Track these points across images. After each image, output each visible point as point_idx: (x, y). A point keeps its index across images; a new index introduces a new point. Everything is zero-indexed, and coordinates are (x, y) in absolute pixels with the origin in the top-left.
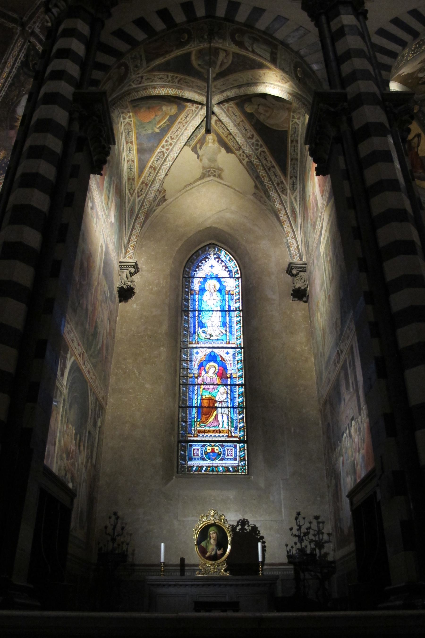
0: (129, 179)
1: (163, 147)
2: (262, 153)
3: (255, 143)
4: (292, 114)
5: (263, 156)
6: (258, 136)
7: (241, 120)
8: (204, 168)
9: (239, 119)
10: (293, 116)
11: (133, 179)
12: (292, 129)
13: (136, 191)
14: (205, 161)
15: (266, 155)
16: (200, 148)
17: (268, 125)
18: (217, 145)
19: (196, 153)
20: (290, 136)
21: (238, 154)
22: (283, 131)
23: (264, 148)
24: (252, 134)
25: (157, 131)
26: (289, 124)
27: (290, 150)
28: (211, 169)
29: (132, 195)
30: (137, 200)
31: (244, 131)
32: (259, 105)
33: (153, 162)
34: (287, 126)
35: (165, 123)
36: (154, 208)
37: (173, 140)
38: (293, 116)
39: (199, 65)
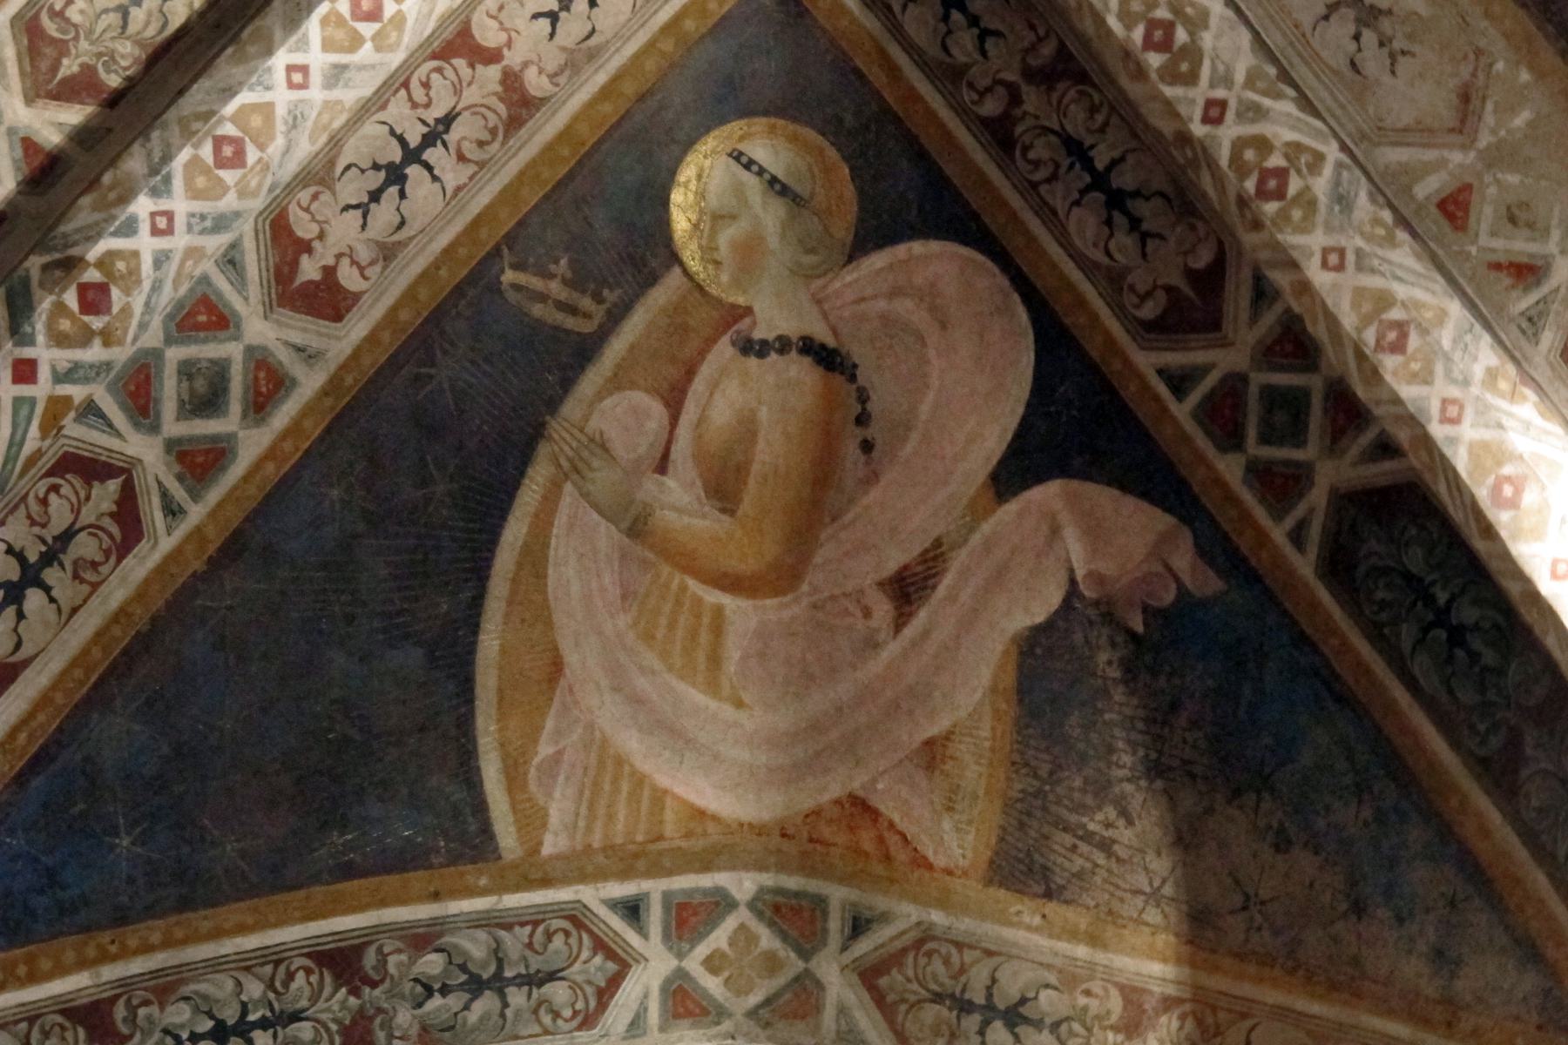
2: (106, 494)
3: (232, 351)
4: (743, 884)
5: (60, 514)
6: (333, 387)
7: (535, 82)
9: (553, 61)
10: (721, 903)
12: (533, 917)
15: (88, 575)
17: (514, 532)
20: (422, 912)
22: (471, 779)
23: (173, 511)
24: (349, 278)
26: (579, 867)
27: (215, 965)
31: (373, 142)
32: (827, 358)
34: (551, 845)
38: (721, 903)
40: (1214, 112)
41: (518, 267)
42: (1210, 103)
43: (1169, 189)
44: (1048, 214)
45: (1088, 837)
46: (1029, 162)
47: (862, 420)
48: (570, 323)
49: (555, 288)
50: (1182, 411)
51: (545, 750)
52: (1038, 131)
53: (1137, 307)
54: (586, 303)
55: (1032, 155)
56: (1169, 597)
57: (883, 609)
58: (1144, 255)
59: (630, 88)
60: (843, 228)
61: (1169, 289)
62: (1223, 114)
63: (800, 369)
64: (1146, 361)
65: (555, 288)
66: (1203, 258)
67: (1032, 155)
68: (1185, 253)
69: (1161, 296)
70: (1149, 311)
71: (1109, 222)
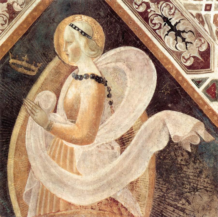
7: (17, 8)
32: (98, 79)
40: (208, 8)
41: (14, 58)
42: (207, 5)
43: (193, 30)
44: (159, 38)
45: (177, 208)
46: (153, 24)
47: (109, 96)
48: (29, 73)
49: (24, 63)
50: (200, 91)
51: (27, 189)
52: (155, 15)
53: (185, 62)
54: (33, 67)
55: (153, 22)
56: (198, 142)
57: (117, 147)
58: (187, 48)
59: (42, 8)
60: (102, 44)
61: (194, 57)
62: (211, 8)
63: (92, 83)
64: (189, 77)
65: (24, 63)
66: (204, 48)
67: (153, 22)
68: (198, 47)
69: (192, 59)
70: (188, 64)
71: (176, 40)
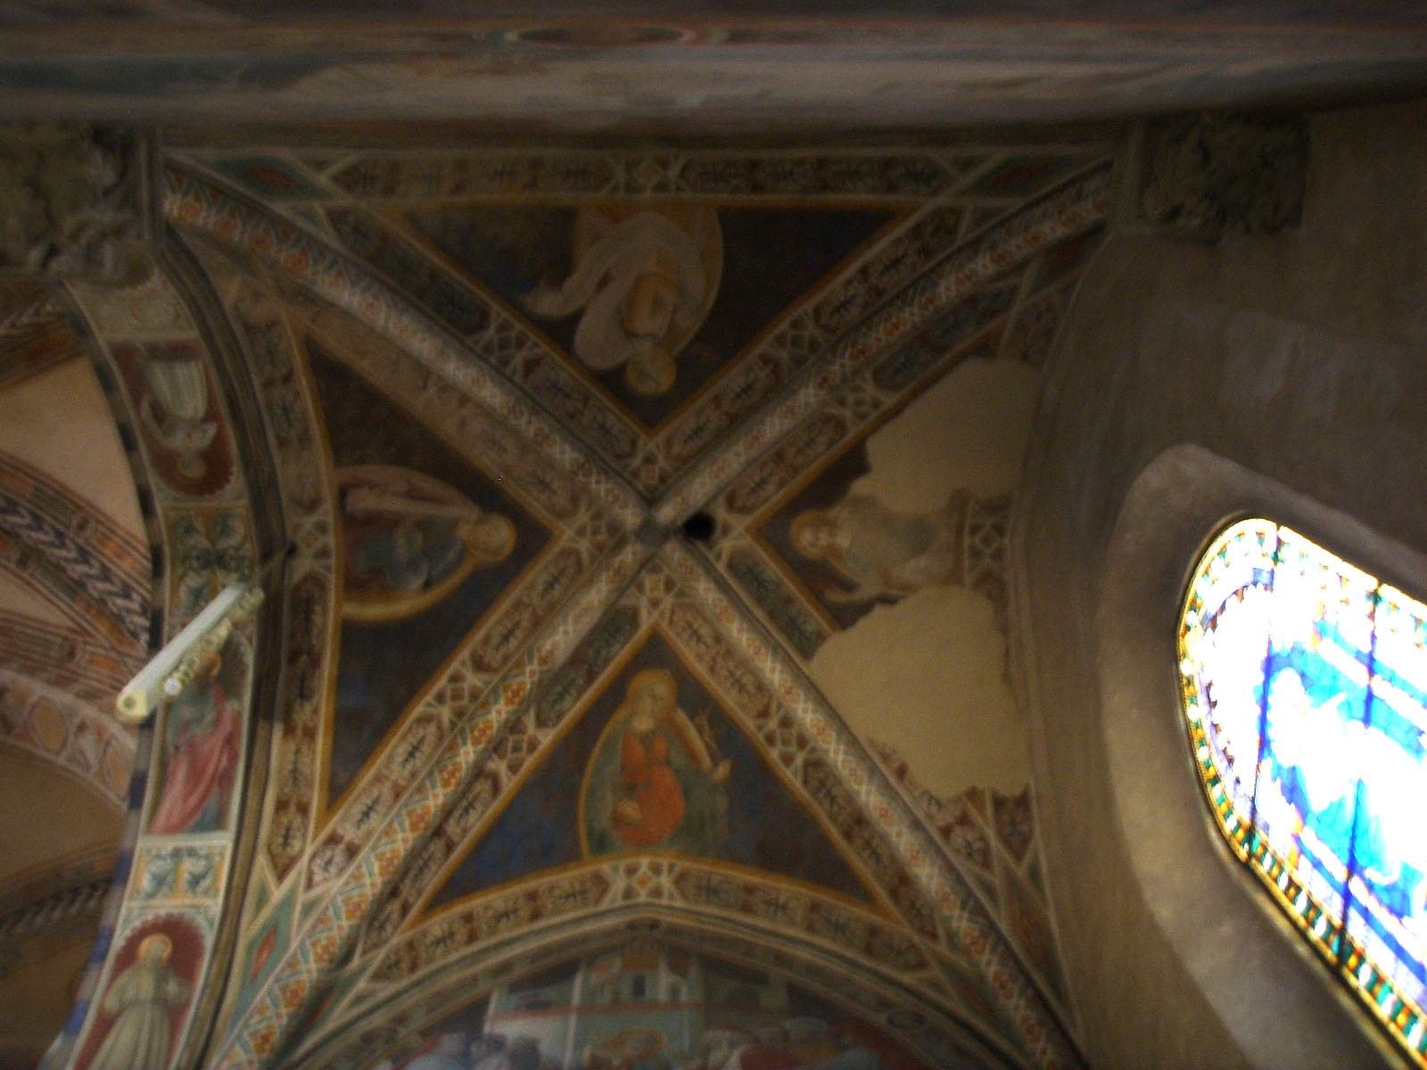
0: (869, 951)
1: (788, 760)
8: (952, 577)
11: (874, 931)
13: (916, 939)
14: (912, 569)
16: (849, 587)
17: (714, 294)
18: (838, 512)
19: (865, 608)
21: (862, 426)
25: (723, 770)
28: (967, 541)
29: (921, 965)
30: (942, 947)
33: (833, 818)
35: (700, 730)
36: (1021, 872)
37: (774, 707)
39: (428, 585)
